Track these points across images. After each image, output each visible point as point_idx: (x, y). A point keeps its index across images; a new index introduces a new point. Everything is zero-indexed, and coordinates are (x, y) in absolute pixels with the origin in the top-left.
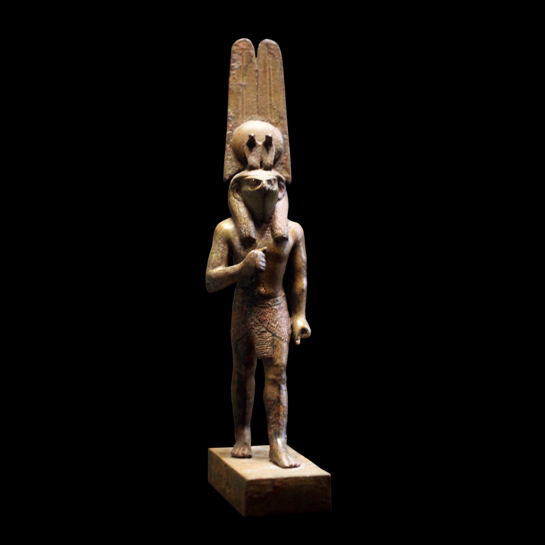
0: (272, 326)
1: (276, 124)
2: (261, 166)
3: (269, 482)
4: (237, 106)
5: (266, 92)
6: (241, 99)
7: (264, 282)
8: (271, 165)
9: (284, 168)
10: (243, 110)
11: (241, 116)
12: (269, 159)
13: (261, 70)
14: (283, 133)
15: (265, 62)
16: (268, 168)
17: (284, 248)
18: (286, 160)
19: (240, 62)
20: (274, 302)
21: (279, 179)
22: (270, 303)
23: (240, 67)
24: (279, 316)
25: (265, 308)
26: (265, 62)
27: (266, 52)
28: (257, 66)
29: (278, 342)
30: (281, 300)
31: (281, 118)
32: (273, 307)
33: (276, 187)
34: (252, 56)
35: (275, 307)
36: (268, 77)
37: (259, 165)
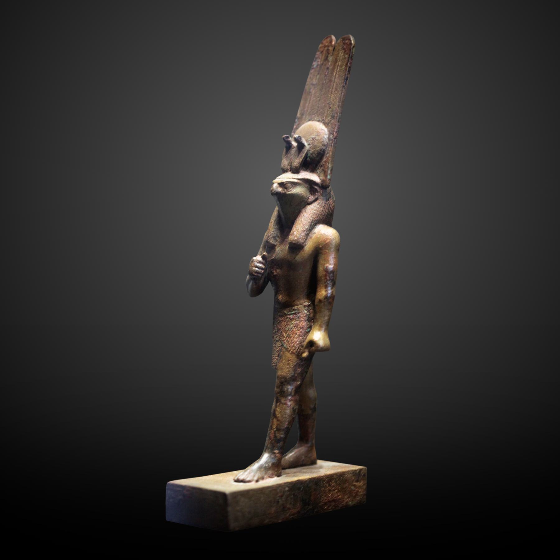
0: (283, 336)
1: (326, 124)
2: (290, 171)
3: (188, 490)
4: (304, 106)
5: (329, 91)
6: (309, 99)
7: (282, 289)
8: (296, 167)
9: (323, 170)
10: (307, 111)
11: (304, 117)
12: (297, 162)
13: (331, 68)
14: (331, 133)
15: (336, 59)
16: (296, 171)
17: (297, 255)
18: (326, 162)
19: (319, 60)
20: (290, 311)
21: (310, 183)
22: (286, 312)
23: (318, 65)
24: (292, 326)
25: (282, 316)
26: (336, 59)
27: (340, 48)
28: (330, 64)
29: (284, 352)
30: (303, 308)
31: (333, 117)
32: (288, 316)
33: (298, 190)
34: (329, 54)
35: (291, 316)
36: (335, 74)
37: (289, 167)
